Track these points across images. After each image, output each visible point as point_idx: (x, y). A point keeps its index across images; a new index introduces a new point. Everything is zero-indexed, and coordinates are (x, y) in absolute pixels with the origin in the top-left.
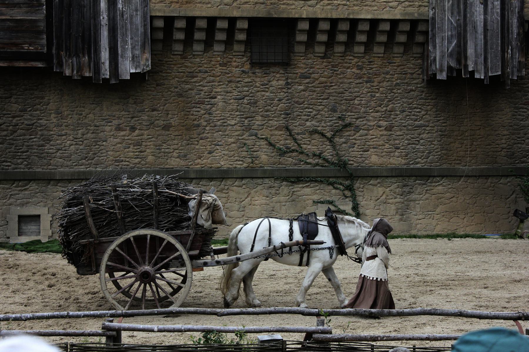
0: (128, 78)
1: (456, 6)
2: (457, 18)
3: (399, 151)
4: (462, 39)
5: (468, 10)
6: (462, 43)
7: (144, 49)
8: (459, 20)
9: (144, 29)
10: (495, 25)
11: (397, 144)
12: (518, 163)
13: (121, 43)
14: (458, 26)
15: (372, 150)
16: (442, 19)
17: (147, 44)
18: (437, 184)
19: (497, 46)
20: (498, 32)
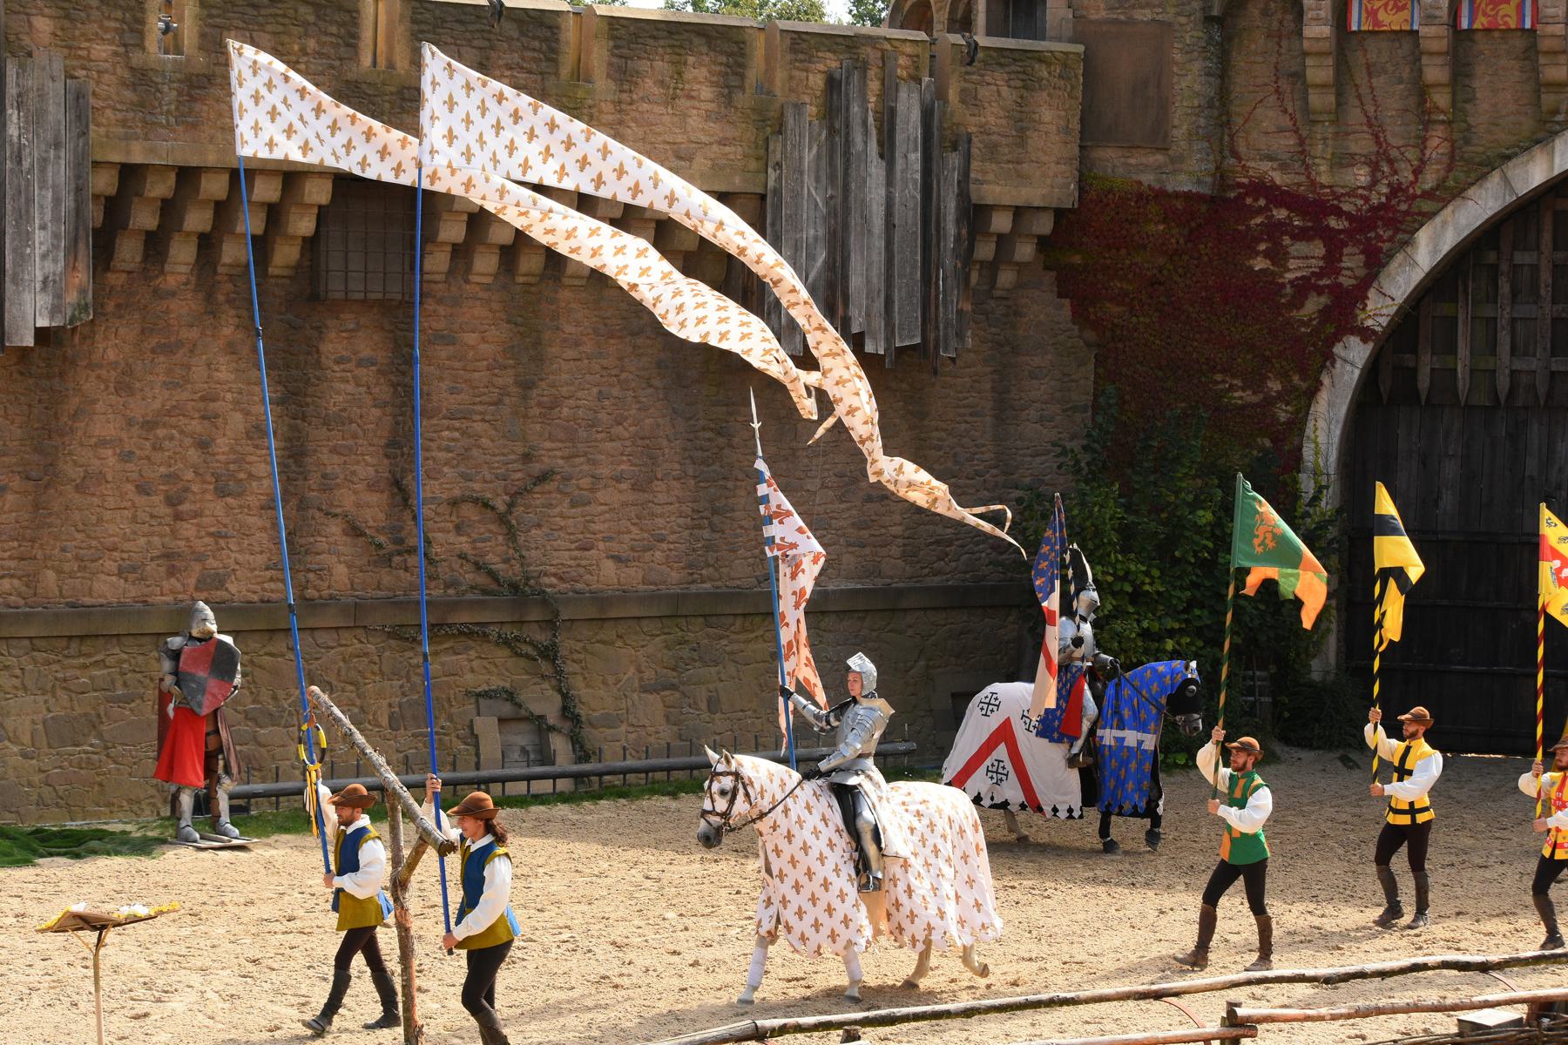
0: (29, 341)
1: (823, 163)
2: (829, 192)
3: (664, 546)
4: (839, 249)
5: (853, 173)
6: (838, 259)
7: (76, 259)
8: (832, 197)
9: (76, 201)
10: (911, 213)
11: (660, 529)
12: (927, 575)
13: (13, 240)
14: (829, 213)
15: (601, 545)
16: (797, 195)
17: (81, 246)
18: (752, 636)
19: (914, 267)
20: (915, 233)
